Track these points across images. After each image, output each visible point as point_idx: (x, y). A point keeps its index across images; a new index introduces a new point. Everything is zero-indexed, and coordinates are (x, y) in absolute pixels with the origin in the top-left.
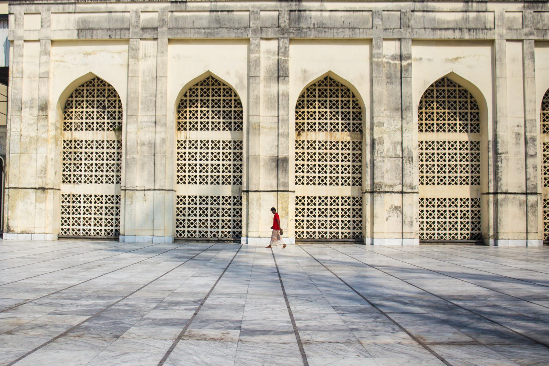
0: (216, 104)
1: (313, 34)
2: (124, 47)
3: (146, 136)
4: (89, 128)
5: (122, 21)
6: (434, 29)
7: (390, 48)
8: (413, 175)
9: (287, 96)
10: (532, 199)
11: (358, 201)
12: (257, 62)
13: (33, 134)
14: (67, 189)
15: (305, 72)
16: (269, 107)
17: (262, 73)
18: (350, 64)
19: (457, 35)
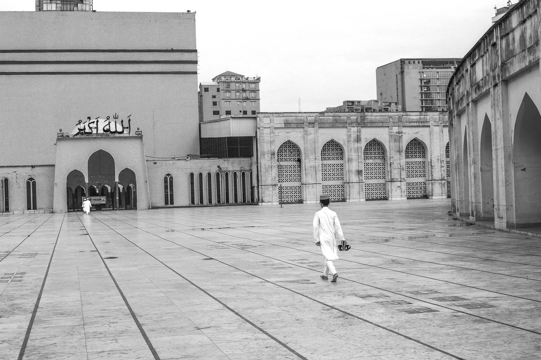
0: (333, 150)
1: (369, 125)
2: (302, 130)
3: (312, 164)
4: (286, 160)
5: (301, 120)
6: (410, 122)
7: (395, 129)
8: (404, 175)
9: (361, 148)
10: (443, 181)
11: (384, 185)
12: (350, 136)
13: (270, 164)
14: (279, 184)
15: (366, 138)
16: (355, 152)
17: (352, 139)
18: (382, 135)
19: (418, 124)
